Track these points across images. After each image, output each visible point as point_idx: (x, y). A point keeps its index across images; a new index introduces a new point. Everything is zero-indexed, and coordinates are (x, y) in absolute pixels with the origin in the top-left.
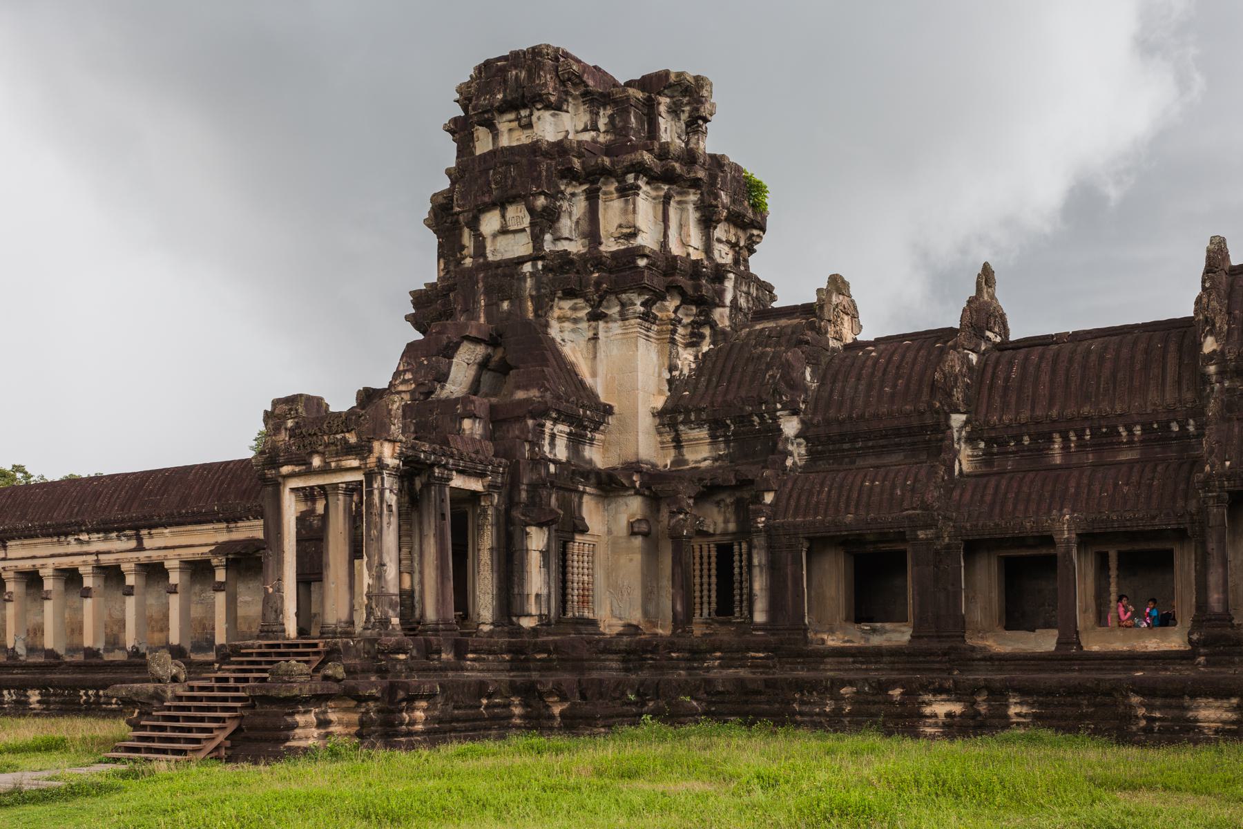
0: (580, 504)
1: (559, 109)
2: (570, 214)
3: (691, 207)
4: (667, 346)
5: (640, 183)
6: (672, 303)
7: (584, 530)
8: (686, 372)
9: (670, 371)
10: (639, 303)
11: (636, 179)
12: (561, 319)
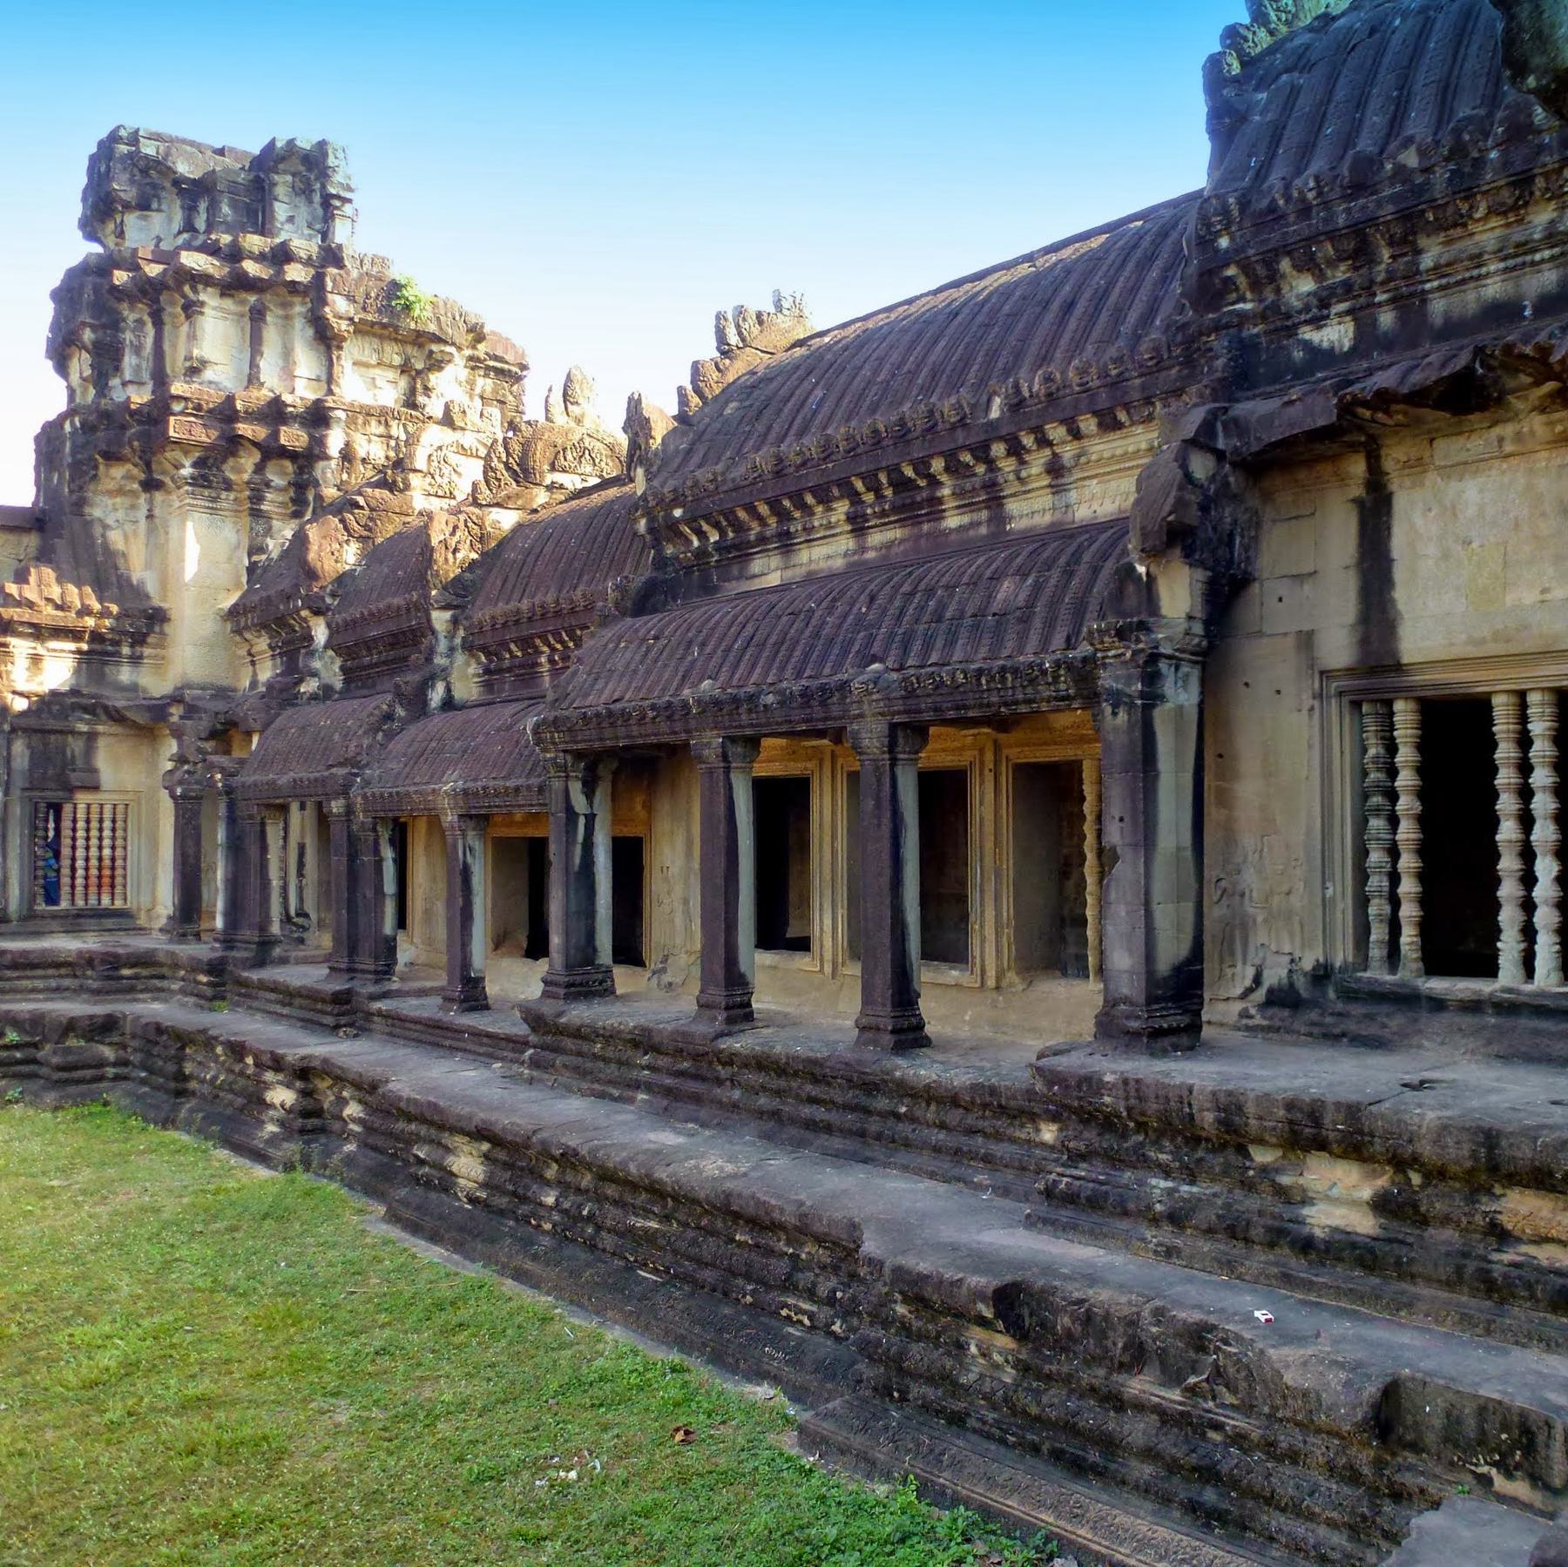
0: (89, 751)
1: (147, 207)
2: (138, 350)
3: (299, 323)
4: (246, 520)
5: (202, 297)
6: (248, 461)
7: (96, 788)
8: (275, 555)
9: (250, 556)
10: (187, 463)
11: (195, 291)
12: (111, 493)
